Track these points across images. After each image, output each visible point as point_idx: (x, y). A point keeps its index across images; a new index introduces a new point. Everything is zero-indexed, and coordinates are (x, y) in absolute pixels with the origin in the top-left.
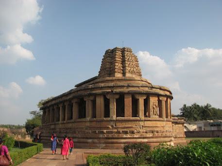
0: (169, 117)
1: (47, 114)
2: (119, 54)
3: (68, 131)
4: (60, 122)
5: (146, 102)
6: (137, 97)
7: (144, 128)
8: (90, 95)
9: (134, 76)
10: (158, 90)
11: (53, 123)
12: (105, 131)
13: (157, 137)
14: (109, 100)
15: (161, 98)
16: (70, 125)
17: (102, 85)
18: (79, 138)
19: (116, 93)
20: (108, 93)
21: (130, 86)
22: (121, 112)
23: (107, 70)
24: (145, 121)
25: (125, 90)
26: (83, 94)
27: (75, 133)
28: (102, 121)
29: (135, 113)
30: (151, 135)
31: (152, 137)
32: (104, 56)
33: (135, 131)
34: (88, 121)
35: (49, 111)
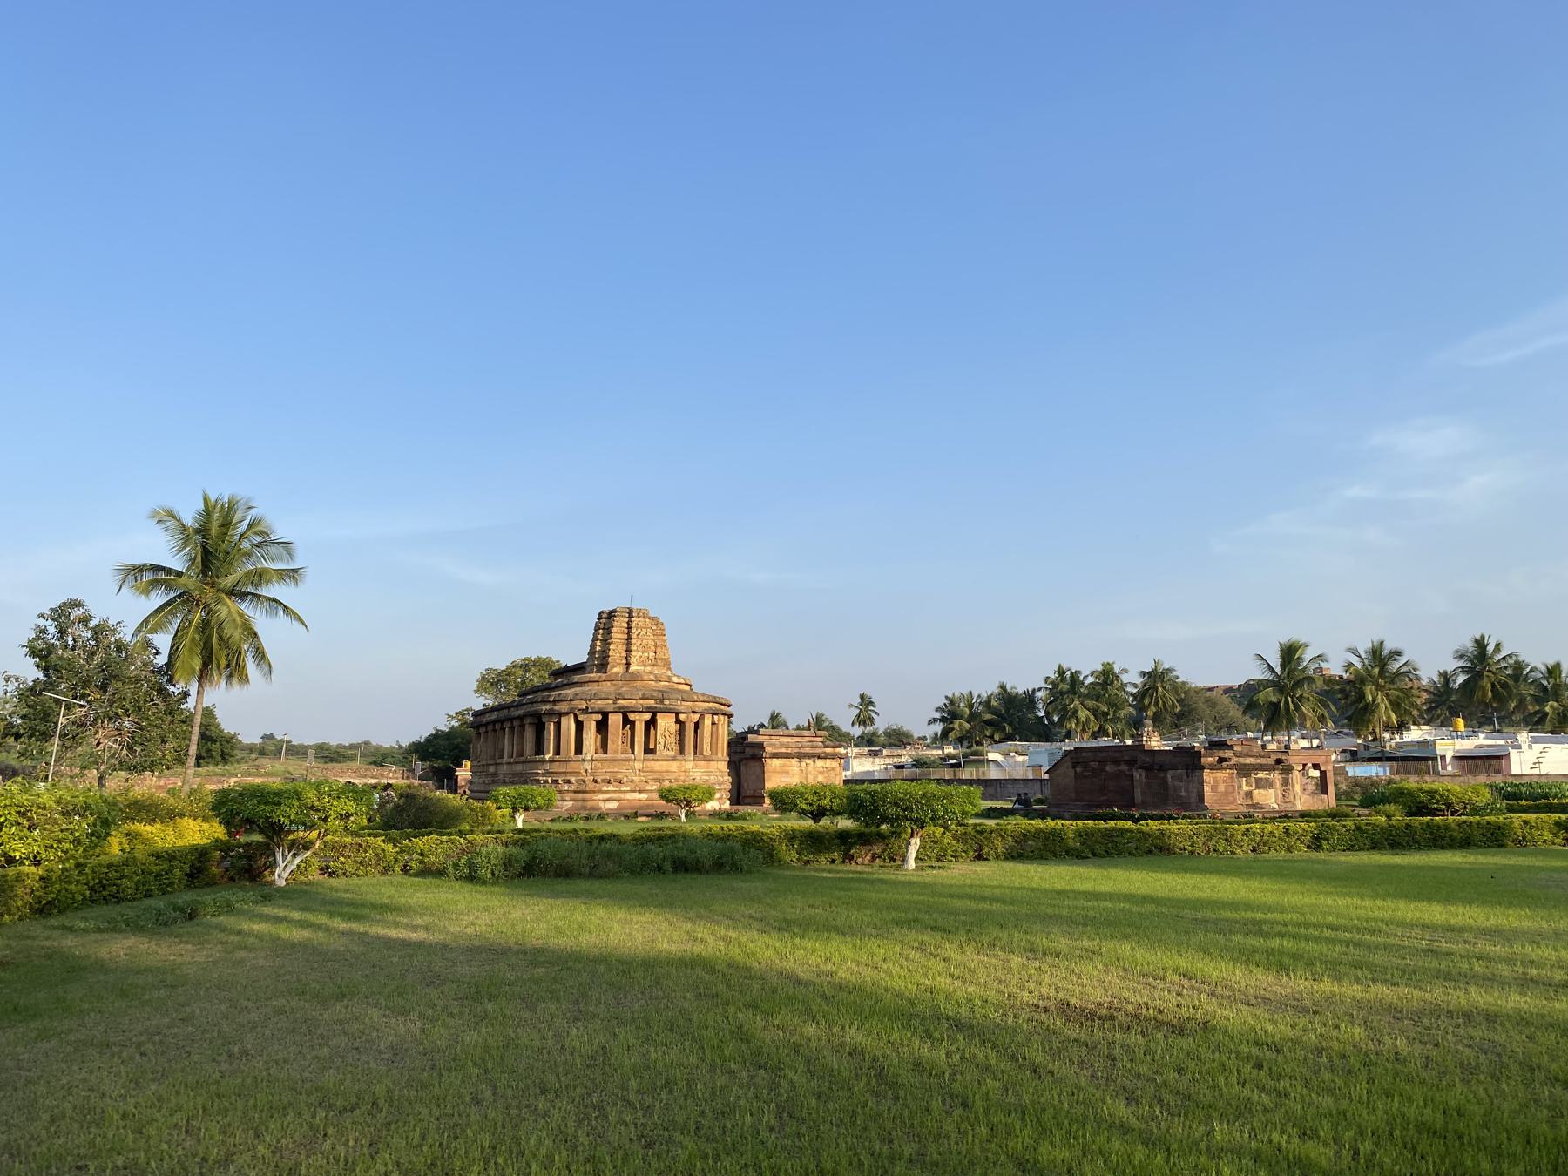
0: (707, 753)
2: (620, 624)
6: (632, 716)
8: (551, 714)
12: (573, 779)
15: (682, 717)
16: (519, 768)
17: (570, 692)
25: (608, 705)
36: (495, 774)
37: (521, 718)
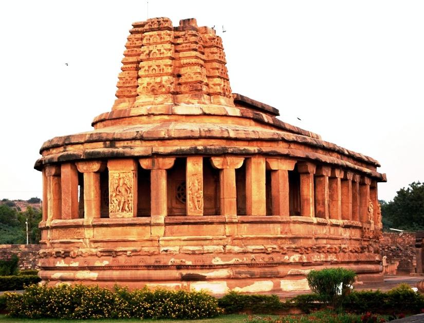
7: (93, 245)
10: (138, 143)
13: (122, 268)
15: (145, 164)
31: (109, 268)
33: (75, 251)
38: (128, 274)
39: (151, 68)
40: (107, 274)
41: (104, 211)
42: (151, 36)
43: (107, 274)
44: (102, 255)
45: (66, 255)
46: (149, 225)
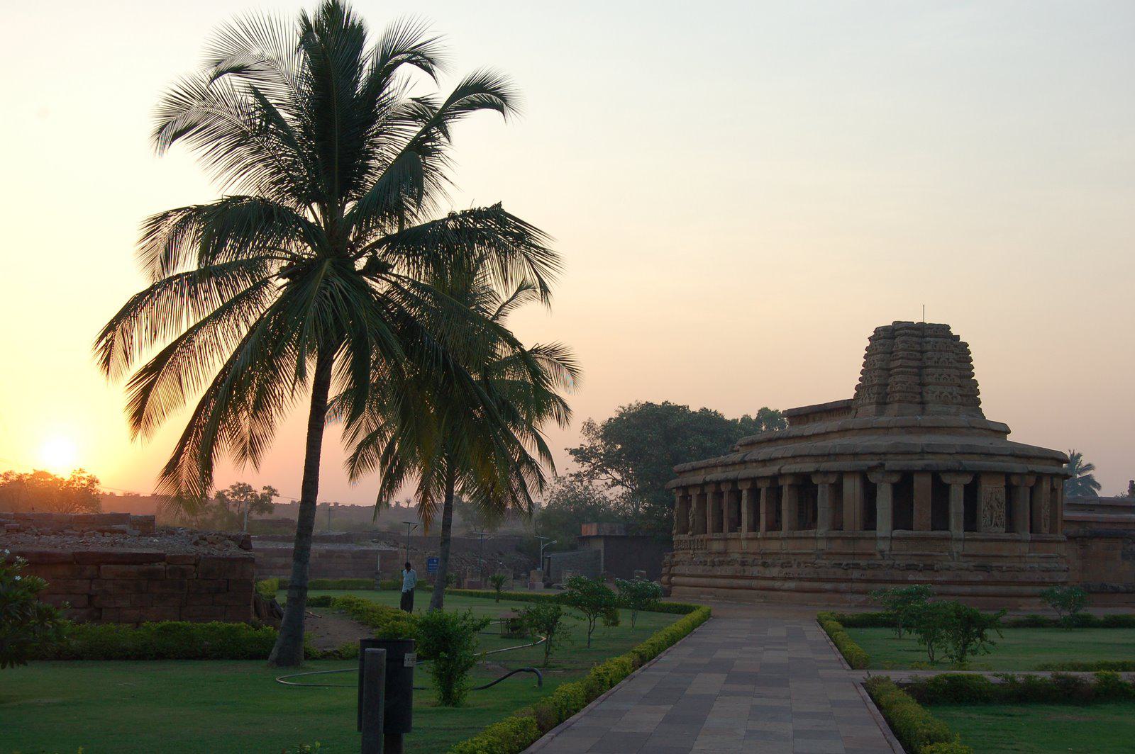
0: (1045, 530)
1: (694, 504)
3: (769, 561)
4: (744, 531)
5: (971, 493)
6: (946, 479)
9: (953, 410)
11: (718, 535)
12: (863, 563)
13: (997, 583)
14: (875, 485)
15: (1014, 480)
16: (774, 546)
18: (800, 579)
19: (892, 472)
20: (872, 469)
21: (928, 453)
22: (902, 518)
23: (875, 390)
24: (965, 540)
26: (812, 470)
27: (791, 566)
28: (860, 538)
29: (940, 518)
30: (980, 577)
32: (870, 338)
34: (823, 538)
35: (702, 496)
36: (725, 553)
37: (775, 478)
38: (1003, 589)
39: (943, 377)
40: (982, 589)
41: (971, 522)
42: (937, 343)
43: (982, 589)
44: (976, 570)
45: (929, 568)
46: (1019, 541)
